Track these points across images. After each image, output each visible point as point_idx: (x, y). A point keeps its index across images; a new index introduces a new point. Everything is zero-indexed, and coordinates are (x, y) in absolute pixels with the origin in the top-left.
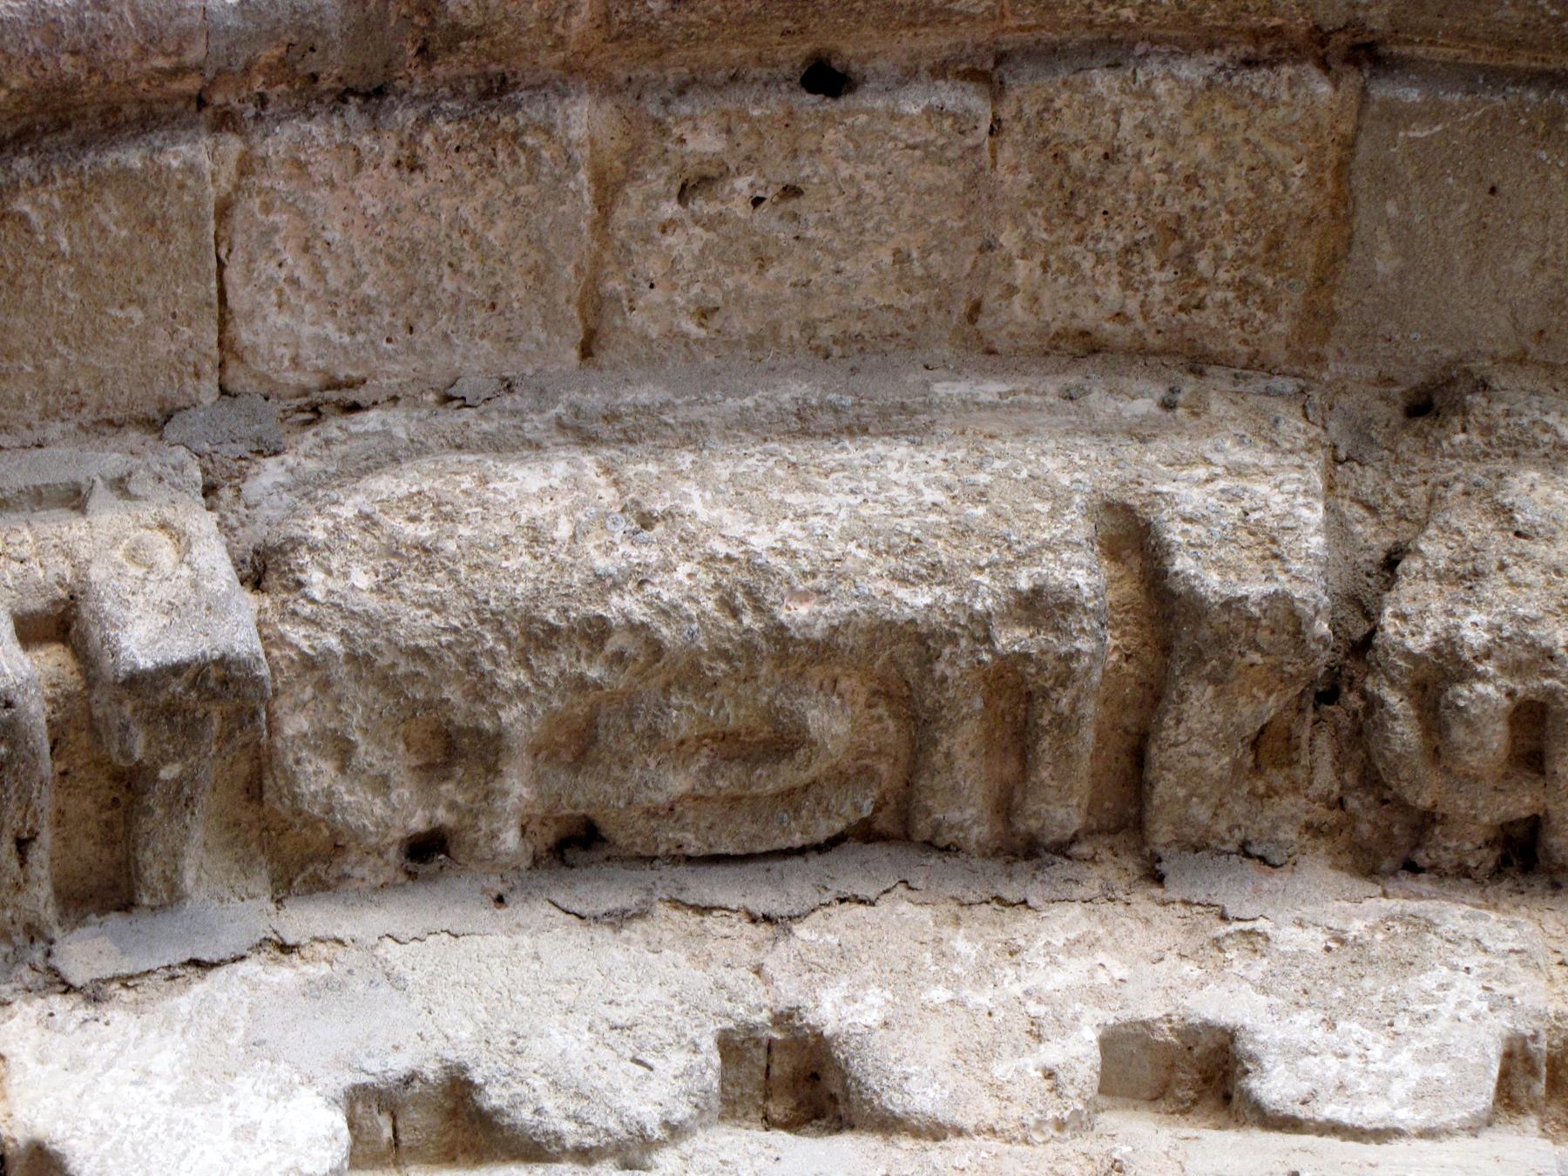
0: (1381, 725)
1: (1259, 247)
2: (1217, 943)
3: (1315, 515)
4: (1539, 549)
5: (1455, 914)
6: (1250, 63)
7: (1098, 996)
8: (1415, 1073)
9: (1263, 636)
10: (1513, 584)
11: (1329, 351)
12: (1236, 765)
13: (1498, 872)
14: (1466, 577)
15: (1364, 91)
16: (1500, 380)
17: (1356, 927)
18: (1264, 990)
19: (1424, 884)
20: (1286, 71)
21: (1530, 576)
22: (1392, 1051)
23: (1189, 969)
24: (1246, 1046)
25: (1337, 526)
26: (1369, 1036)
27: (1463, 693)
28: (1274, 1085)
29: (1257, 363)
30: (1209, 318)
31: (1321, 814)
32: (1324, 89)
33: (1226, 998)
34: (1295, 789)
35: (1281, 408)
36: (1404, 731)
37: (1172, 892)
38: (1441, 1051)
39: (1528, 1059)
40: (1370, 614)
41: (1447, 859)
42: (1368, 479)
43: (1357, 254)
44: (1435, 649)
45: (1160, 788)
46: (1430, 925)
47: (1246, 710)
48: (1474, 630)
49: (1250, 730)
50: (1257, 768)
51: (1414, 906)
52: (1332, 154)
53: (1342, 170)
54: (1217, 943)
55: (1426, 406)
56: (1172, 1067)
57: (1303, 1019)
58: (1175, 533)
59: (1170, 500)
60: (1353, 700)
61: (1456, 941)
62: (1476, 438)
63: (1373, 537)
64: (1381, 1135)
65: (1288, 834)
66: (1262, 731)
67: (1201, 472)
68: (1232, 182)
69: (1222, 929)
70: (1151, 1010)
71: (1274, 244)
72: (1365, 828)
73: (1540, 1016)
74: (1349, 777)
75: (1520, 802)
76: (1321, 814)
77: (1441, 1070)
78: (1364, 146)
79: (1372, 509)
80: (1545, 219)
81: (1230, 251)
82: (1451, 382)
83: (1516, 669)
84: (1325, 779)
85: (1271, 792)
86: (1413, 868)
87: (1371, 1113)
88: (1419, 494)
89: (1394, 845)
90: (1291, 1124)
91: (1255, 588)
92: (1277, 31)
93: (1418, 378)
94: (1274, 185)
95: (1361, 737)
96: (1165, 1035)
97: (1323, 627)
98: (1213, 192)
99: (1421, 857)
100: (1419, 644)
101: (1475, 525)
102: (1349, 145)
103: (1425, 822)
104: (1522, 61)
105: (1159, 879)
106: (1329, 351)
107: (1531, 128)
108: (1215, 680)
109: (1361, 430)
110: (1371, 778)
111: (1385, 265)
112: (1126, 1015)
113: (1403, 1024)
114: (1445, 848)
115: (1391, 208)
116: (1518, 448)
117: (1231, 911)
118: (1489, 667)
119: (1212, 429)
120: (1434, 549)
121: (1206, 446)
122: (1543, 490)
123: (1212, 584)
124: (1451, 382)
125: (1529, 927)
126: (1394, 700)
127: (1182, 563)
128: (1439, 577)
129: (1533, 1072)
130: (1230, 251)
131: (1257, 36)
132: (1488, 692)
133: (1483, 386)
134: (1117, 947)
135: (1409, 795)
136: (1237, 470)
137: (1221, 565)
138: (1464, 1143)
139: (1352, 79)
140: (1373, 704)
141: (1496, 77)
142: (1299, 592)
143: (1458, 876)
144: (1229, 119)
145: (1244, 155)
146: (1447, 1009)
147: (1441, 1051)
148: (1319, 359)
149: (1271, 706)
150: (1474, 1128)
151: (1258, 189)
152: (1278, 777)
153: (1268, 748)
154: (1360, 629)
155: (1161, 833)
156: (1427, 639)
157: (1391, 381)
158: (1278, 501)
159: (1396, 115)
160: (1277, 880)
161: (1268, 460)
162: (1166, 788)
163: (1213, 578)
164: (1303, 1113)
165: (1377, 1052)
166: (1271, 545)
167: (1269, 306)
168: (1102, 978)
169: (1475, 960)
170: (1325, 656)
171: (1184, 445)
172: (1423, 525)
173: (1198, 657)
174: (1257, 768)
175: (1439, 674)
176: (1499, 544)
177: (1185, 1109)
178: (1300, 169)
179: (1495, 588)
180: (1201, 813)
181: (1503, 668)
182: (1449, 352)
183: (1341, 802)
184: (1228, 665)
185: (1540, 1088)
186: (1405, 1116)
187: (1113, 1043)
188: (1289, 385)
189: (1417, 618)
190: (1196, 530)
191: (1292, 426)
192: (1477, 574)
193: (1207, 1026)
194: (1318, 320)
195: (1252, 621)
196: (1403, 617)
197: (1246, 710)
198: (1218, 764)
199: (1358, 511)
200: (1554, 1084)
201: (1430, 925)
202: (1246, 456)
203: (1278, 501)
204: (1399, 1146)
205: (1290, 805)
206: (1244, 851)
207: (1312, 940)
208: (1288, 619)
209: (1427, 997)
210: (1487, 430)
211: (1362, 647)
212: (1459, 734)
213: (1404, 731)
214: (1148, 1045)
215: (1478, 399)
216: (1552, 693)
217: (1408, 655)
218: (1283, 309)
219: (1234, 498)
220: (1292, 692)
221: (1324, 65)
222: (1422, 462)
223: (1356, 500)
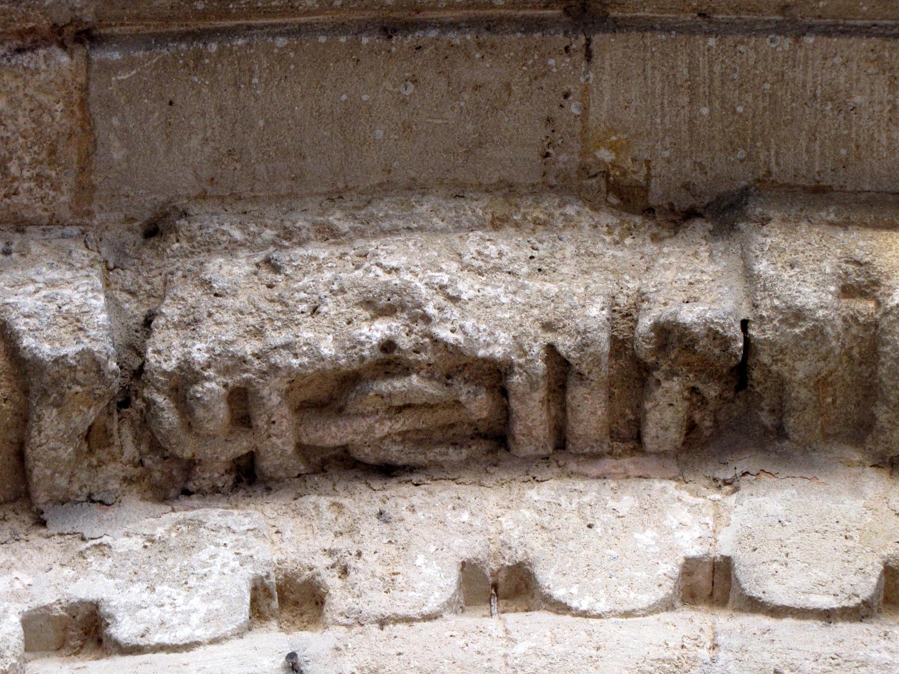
0: (155, 416)
1: (44, 155)
2: (81, 554)
3: (100, 302)
4: (229, 302)
5: (214, 515)
6: (20, 51)
7: (16, 596)
8: (203, 608)
9: (80, 376)
10: (217, 324)
11: (94, 207)
12: (78, 452)
13: (236, 487)
14: (190, 324)
15: (88, 56)
16: (194, 209)
17: (160, 532)
18: (111, 576)
19: (195, 501)
20: (42, 52)
21: (226, 318)
22: (188, 598)
23: (68, 572)
24: (105, 610)
25: (113, 306)
26: (174, 592)
27: (199, 390)
28: (124, 630)
29: (55, 221)
30: (23, 199)
31: (131, 471)
32: (65, 59)
33: (91, 584)
34: (115, 460)
35: (73, 245)
36: (169, 417)
37: (52, 529)
38: (216, 594)
39: (266, 589)
40: (140, 354)
41: (206, 485)
42: (128, 277)
43: (100, 150)
44: (179, 367)
45: (36, 472)
46: (201, 523)
47: (77, 419)
48: (199, 353)
49: (83, 429)
50: (91, 451)
51: (190, 514)
52: (76, 96)
53: (84, 104)
54: (81, 554)
55: (154, 231)
56: (65, 629)
57: (136, 588)
58: (20, 325)
59: (15, 306)
60: (139, 404)
61: (216, 530)
62: (185, 245)
63: (136, 309)
64: (188, 647)
65: (114, 485)
66: (90, 429)
67: (31, 288)
68: (21, 120)
69: (83, 546)
70: (48, 599)
71: (52, 152)
72: (157, 475)
73: (269, 564)
74: (144, 447)
75: (241, 446)
76: (131, 471)
77: (217, 604)
78: (93, 89)
79: (133, 294)
80: (203, 115)
81: (27, 159)
82: (167, 215)
83: (226, 371)
84: (130, 450)
85: (101, 463)
86: (187, 493)
87: (182, 635)
88: (158, 281)
89: (174, 481)
90: (136, 650)
91: (71, 349)
92: (32, 30)
93: (148, 215)
94: (46, 118)
95: (146, 423)
96: (59, 612)
97: (113, 365)
98: (11, 127)
99: (191, 486)
100: (170, 366)
101: (191, 293)
102: (85, 89)
103: (190, 466)
104: (175, 28)
105: (43, 524)
106: (94, 207)
107: (186, 65)
108: (57, 405)
109: (120, 251)
110: (155, 446)
111: (118, 155)
112: (34, 604)
113: (193, 582)
114: (203, 478)
115: (115, 121)
116: (210, 247)
117: (87, 536)
118: (210, 372)
119: (34, 261)
120: (170, 311)
121: (31, 273)
122: (226, 268)
123: (46, 350)
124: (167, 215)
125: (257, 515)
126: (160, 400)
127: (27, 341)
128: (176, 326)
129: (270, 596)
130: (27, 159)
131: (21, 34)
132: (212, 387)
133: (185, 214)
134: (24, 566)
135: (178, 452)
136: (51, 284)
137: (50, 339)
138: (236, 642)
139: (80, 52)
140: (150, 403)
141: (161, 39)
142: (96, 347)
143: (213, 493)
144: (13, 84)
145: (25, 103)
146: (216, 569)
147: (216, 594)
148: (89, 213)
149: (92, 415)
150: (240, 634)
151: (37, 121)
152: (103, 454)
153: (94, 439)
154: (136, 363)
155: (41, 497)
156: (174, 362)
157: (133, 220)
158: (77, 298)
159: (108, 68)
160: (111, 513)
161: (68, 275)
162: (39, 471)
163: (46, 348)
164: (142, 642)
165: (180, 600)
166: (77, 323)
167: (56, 187)
168: (18, 585)
169: (229, 539)
170: (117, 381)
171: (19, 274)
172: (162, 298)
173: (45, 393)
174: (91, 451)
175: (183, 382)
176: (206, 302)
177: (77, 652)
178: (60, 107)
179: (208, 328)
180: (62, 482)
181: (218, 372)
182: (162, 198)
183: (141, 463)
184: (62, 395)
185: (275, 604)
186: (201, 634)
187: (29, 622)
188: (75, 230)
189: (166, 352)
190: (32, 322)
191: (80, 253)
192: (196, 321)
193: (82, 602)
194: (85, 191)
195: (72, 368)
196: (159, 352)
197: (77, 419)
198: (67, 452)
199: (125, 296)
200: (282, 600)
201: (201, 523)
202: (55, 275)
203: (77, 298)
204: (199, 651)
205: (113, 469)
206: (90, 499)
207: (135, 543)
208: (92, 363)
209: (204, 564)
210: (191, 239)
211: (139, 373)
212: (200, 413)
213: (169, 417)
214: (50, 619)
215: (183, 222)
216: (248, 381)
217: (164, 373)
218: (64, 188)
219: (52, 300)
220: (102, 405)
221: (63, 45)
222: (157, 263)
223: (123, 290)
